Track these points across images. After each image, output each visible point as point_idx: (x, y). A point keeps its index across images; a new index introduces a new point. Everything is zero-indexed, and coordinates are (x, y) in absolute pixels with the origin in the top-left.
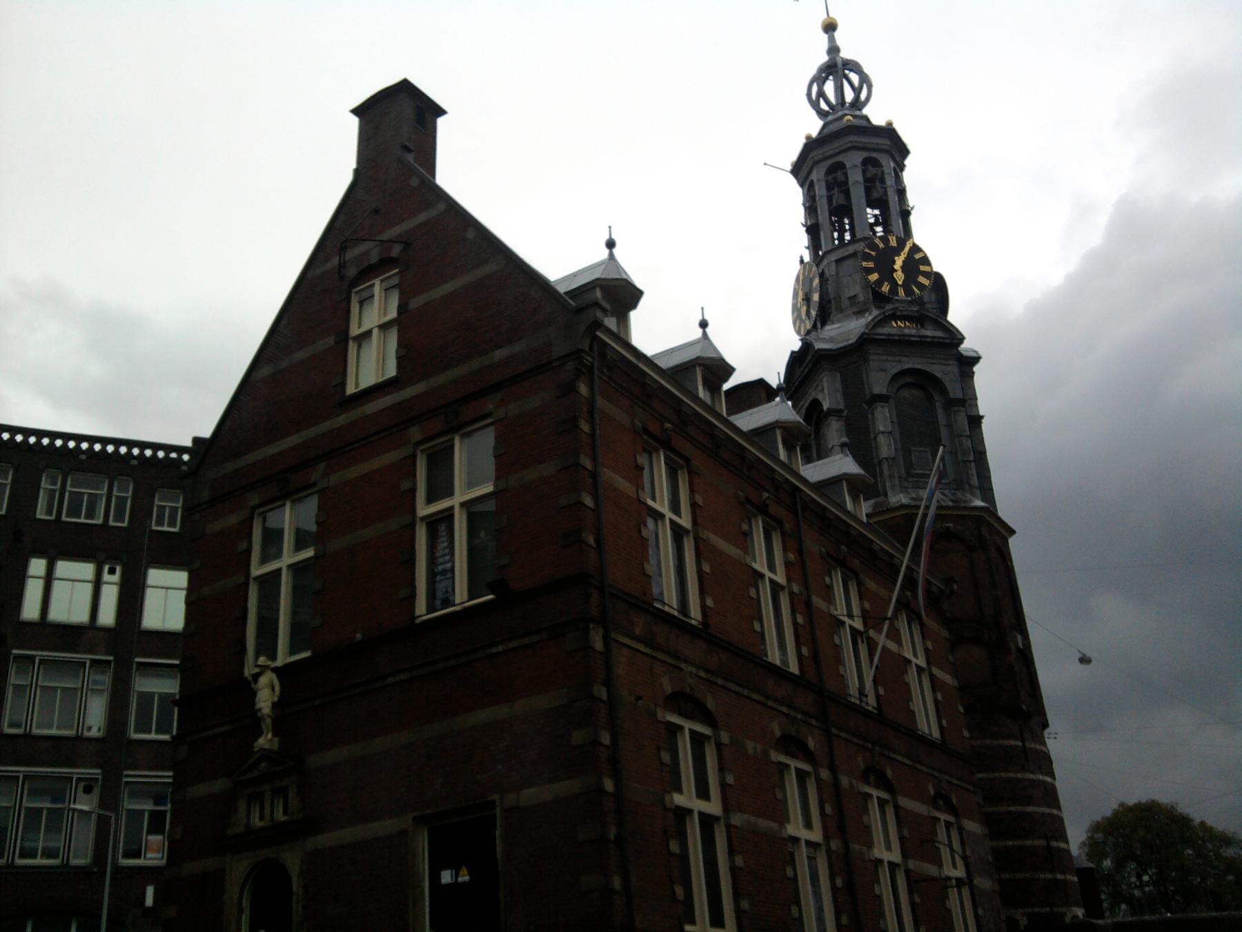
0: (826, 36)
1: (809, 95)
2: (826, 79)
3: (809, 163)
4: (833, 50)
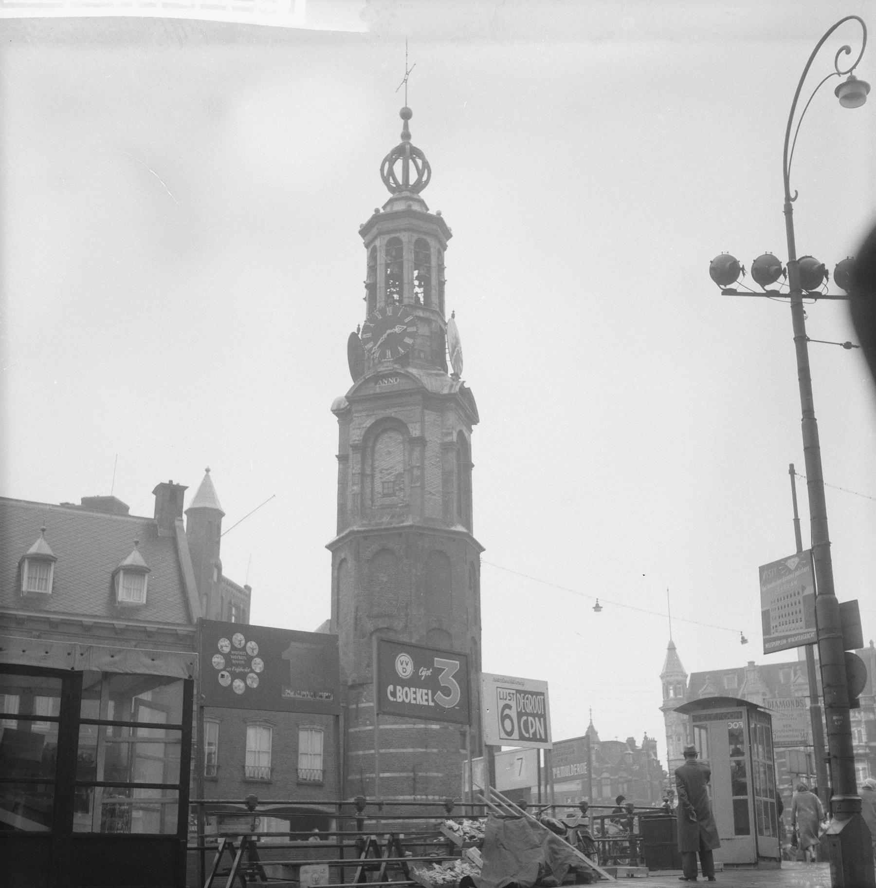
0: (403, 121)
1: (382, 170)
2: (396, 159)
3: (375, 231)
4: (406, 136)
